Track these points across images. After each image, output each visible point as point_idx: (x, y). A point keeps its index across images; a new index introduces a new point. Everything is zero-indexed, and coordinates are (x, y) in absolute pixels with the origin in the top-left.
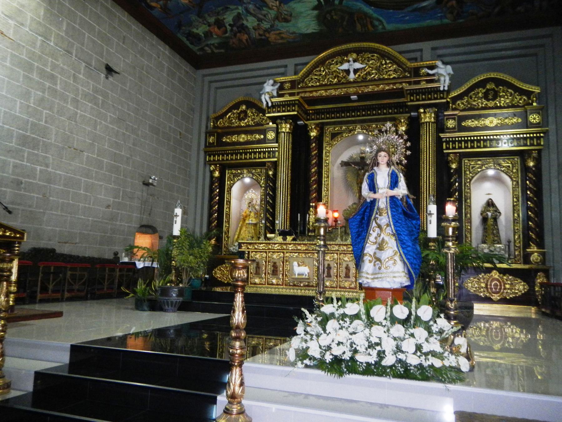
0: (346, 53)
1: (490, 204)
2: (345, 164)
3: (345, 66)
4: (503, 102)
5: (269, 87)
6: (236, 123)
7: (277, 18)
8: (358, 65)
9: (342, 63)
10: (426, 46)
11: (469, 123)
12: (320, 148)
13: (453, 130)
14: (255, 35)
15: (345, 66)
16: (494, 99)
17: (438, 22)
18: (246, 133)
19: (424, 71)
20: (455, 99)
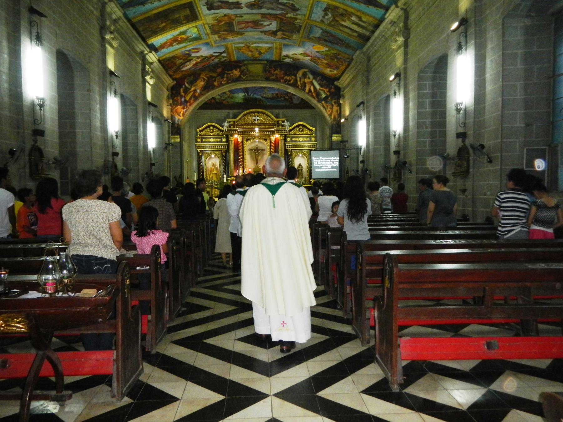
0: (254, 112)
1: (300, 165)
2: (251, 150)
3: (254, 118)
4: (304, 133)
5: (226, 124)
6: (209, 133)
7: (228, 97)
8: (258, 118)
9: (252, 117)
10: (281, 111)
11: (294, 139)
12: (243, 145)
13: (289, 142)
14: (217, 100)
15: (254, 118)
16: (302, 131)
17: (284, 104)
18: (214, 138)
19: (280, 122)
20: (290, 130)
